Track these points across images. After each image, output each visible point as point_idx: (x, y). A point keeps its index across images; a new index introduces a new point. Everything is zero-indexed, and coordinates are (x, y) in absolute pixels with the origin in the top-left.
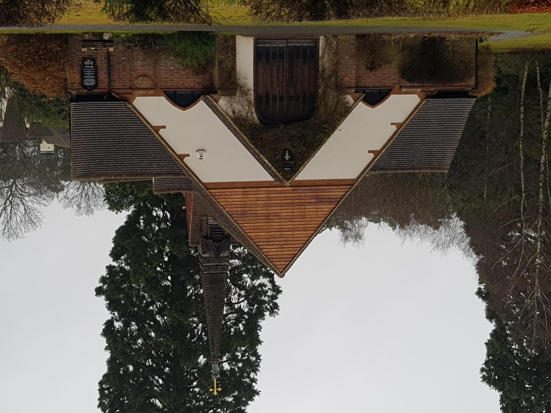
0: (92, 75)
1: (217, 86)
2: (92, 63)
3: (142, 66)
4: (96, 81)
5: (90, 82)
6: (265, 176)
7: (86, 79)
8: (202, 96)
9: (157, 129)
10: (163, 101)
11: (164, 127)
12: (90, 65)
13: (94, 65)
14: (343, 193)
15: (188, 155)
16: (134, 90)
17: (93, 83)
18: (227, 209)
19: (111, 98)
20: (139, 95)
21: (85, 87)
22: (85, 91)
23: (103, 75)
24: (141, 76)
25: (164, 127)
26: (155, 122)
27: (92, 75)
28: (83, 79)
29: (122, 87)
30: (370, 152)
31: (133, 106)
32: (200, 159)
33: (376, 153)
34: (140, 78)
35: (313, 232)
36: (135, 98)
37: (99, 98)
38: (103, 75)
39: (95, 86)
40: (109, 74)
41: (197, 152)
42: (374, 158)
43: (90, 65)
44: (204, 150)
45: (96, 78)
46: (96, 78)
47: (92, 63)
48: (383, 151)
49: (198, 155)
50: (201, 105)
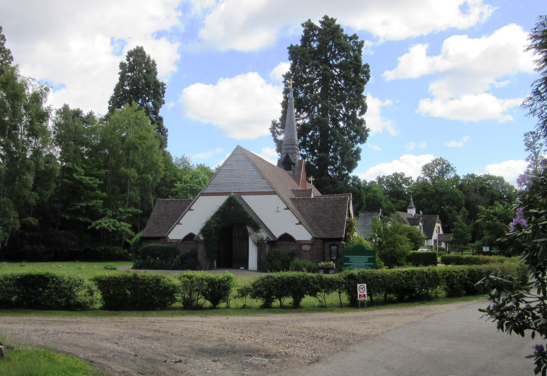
1: (267, 245)
2: (332, 258)
3: (307, 256)
4: (330, 248)
5: (334, 248)
6: (246, 198)
9: (300, 223)
10: (297, 238)
11: (296, 224)
12: (333, 257)
13: (331, 257)
14: (207, 189)
15: (284, 209)
17: (332, 247)
18: (265, 181)
21: (336, 245)
22: (336, 244)
23: (327, 251)
25: (296, 224)
26: (301, 226)
28: (337, 250)
30: (193, 210)
31: (312, 235)
33: (190, 209)
34: (308, 250)
35: (222, 169)
36: (311, 239)
37: (329, 240)
38: (327, 251)
40: (324, 252)
42: (191, 207)
43: (333, 257)
46: (330, 250)
47: (332, 258)
48: (186, 210)
49: (279, 209)
50: (277, 235)
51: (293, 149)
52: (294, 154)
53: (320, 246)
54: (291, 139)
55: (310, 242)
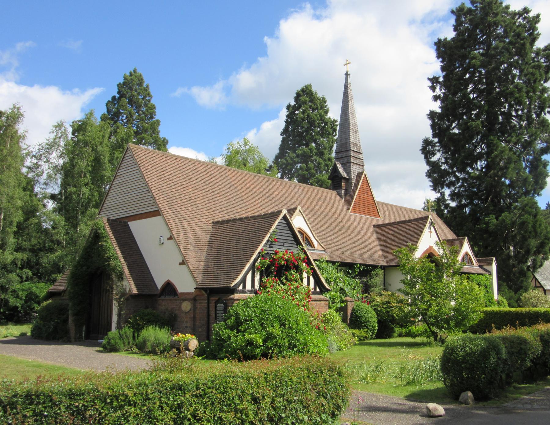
0: (219, 314)
7: (222, 310)
8: (158, 293)
16: (194, 299)
19: (205, 289)
20: (193, 293)
24: (188, 312)
27: (219, 314)
29: (202, 301)
32: (162, 237)
34: (188, 311)
39: (217, 302)
41: (163, 243)
44: (160, 244)
45: (216, 310)
50: (160, 284)
51: (347, 158)
52: (348, 165)
53: (205, 303)
54: (346, 143)
55: (192, 297)
